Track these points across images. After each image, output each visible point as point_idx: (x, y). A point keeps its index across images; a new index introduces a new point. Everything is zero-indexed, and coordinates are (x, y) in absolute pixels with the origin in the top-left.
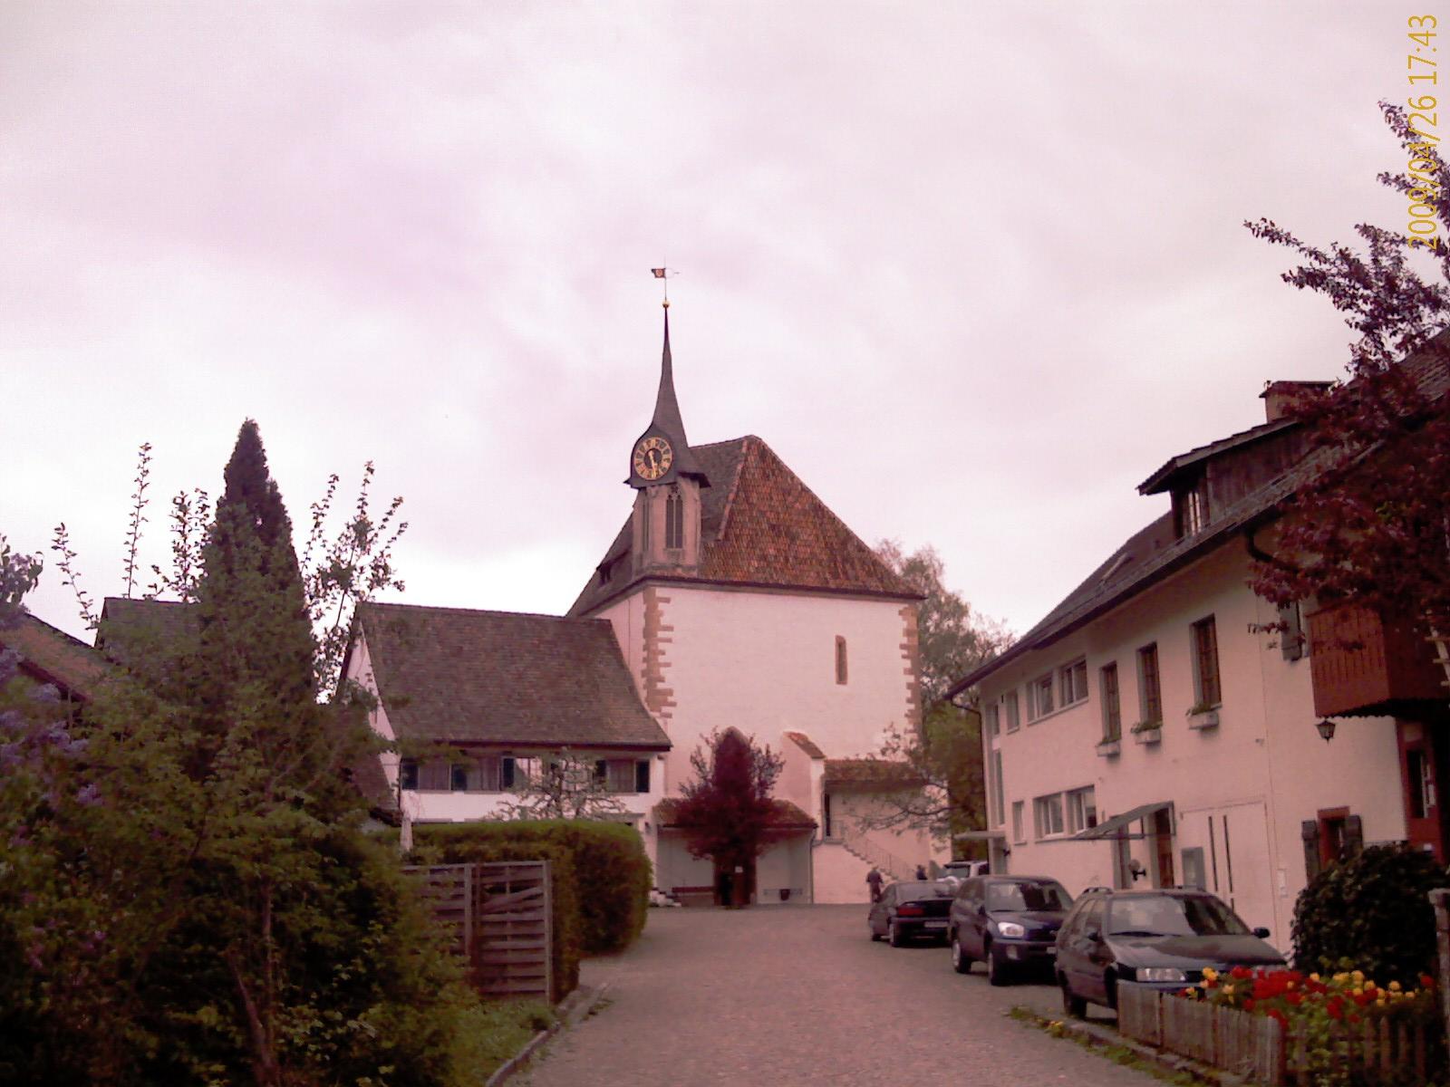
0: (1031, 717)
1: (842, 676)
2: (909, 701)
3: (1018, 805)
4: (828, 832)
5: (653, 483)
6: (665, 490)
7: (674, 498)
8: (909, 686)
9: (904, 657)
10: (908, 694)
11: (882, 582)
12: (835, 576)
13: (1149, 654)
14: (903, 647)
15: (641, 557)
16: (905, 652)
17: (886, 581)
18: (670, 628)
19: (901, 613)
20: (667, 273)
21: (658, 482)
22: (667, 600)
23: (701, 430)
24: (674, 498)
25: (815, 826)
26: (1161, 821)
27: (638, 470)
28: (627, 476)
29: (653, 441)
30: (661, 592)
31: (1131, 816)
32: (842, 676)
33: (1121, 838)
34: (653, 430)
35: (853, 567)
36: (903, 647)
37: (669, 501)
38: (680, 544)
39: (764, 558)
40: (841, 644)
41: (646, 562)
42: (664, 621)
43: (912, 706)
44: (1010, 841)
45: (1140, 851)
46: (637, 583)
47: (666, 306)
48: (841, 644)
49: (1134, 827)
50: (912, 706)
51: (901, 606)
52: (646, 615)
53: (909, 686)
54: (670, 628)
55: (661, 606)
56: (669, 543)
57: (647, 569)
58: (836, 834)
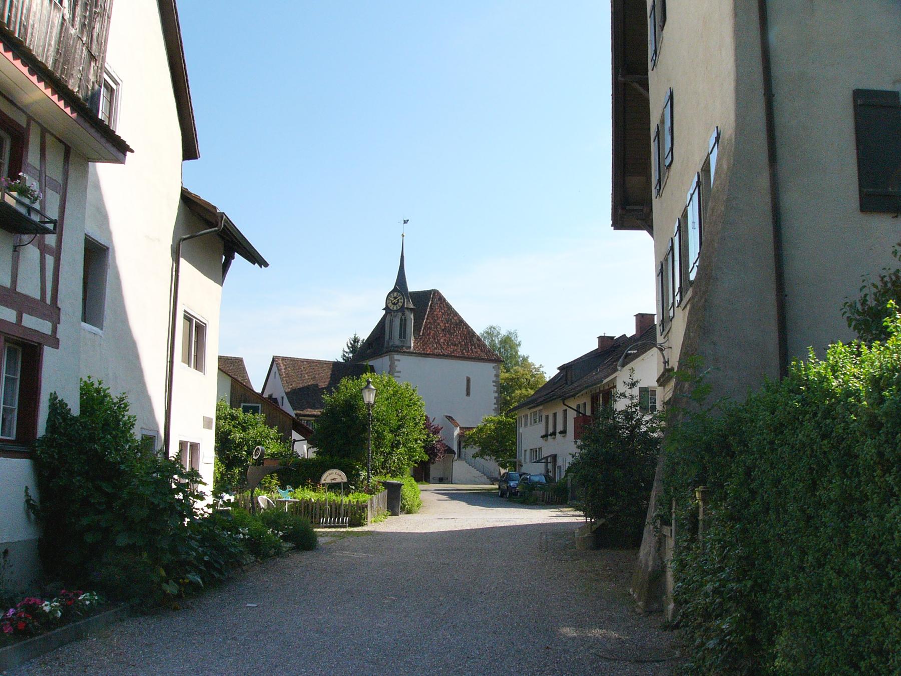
0: (531, 424)
1: (468, 394)
2: (495, 404)
3: (525, 451)
4: (459, 456)
5: (395, 311)
6: (400, 314)
7: (403, 318)
8: (495, 398)
9: (494, 386)
10: (495, 401)
11: (486, 354)
12: (468, 352)
13: (555, 414)
14: (493, 382)
15: (388, 343)
16: (494, 384)
17: (488, 354)
18: (400, 372)
19: (493, 367)
20: (403, 222)
21: (397, 311)
22: (399, 360)
23: (413, 286)
24: (403, 318)
25: (455, 454)
26: (554, 457)
27: (389, 305)
28: (384, 307)
29: (396, 294)
30: (396, 357)
31: (549, 456)
32: (468, 394)
33: (547, 463)
34: (395, 290)
35: (475, 348)
36: (493, 382)
37: (401, 320)
38: (405, 338)
39: (439, 343)
40: (468, 380)
41: (391, 344)
42: (397, 369)
43: (496, 406)
44: (523, 461)
45: (550, 466)
46: (387, 352)
47: (403, 236)
48: (468, 380)
49: (549, 461)
50: (496, 406)
51: (494, 365)
52: (390, 366)
53: (495, 398)
54: (400, 372)
55: (396, 363)
56: (400, 337)
57: (392, 346)
58: (462, 456)
